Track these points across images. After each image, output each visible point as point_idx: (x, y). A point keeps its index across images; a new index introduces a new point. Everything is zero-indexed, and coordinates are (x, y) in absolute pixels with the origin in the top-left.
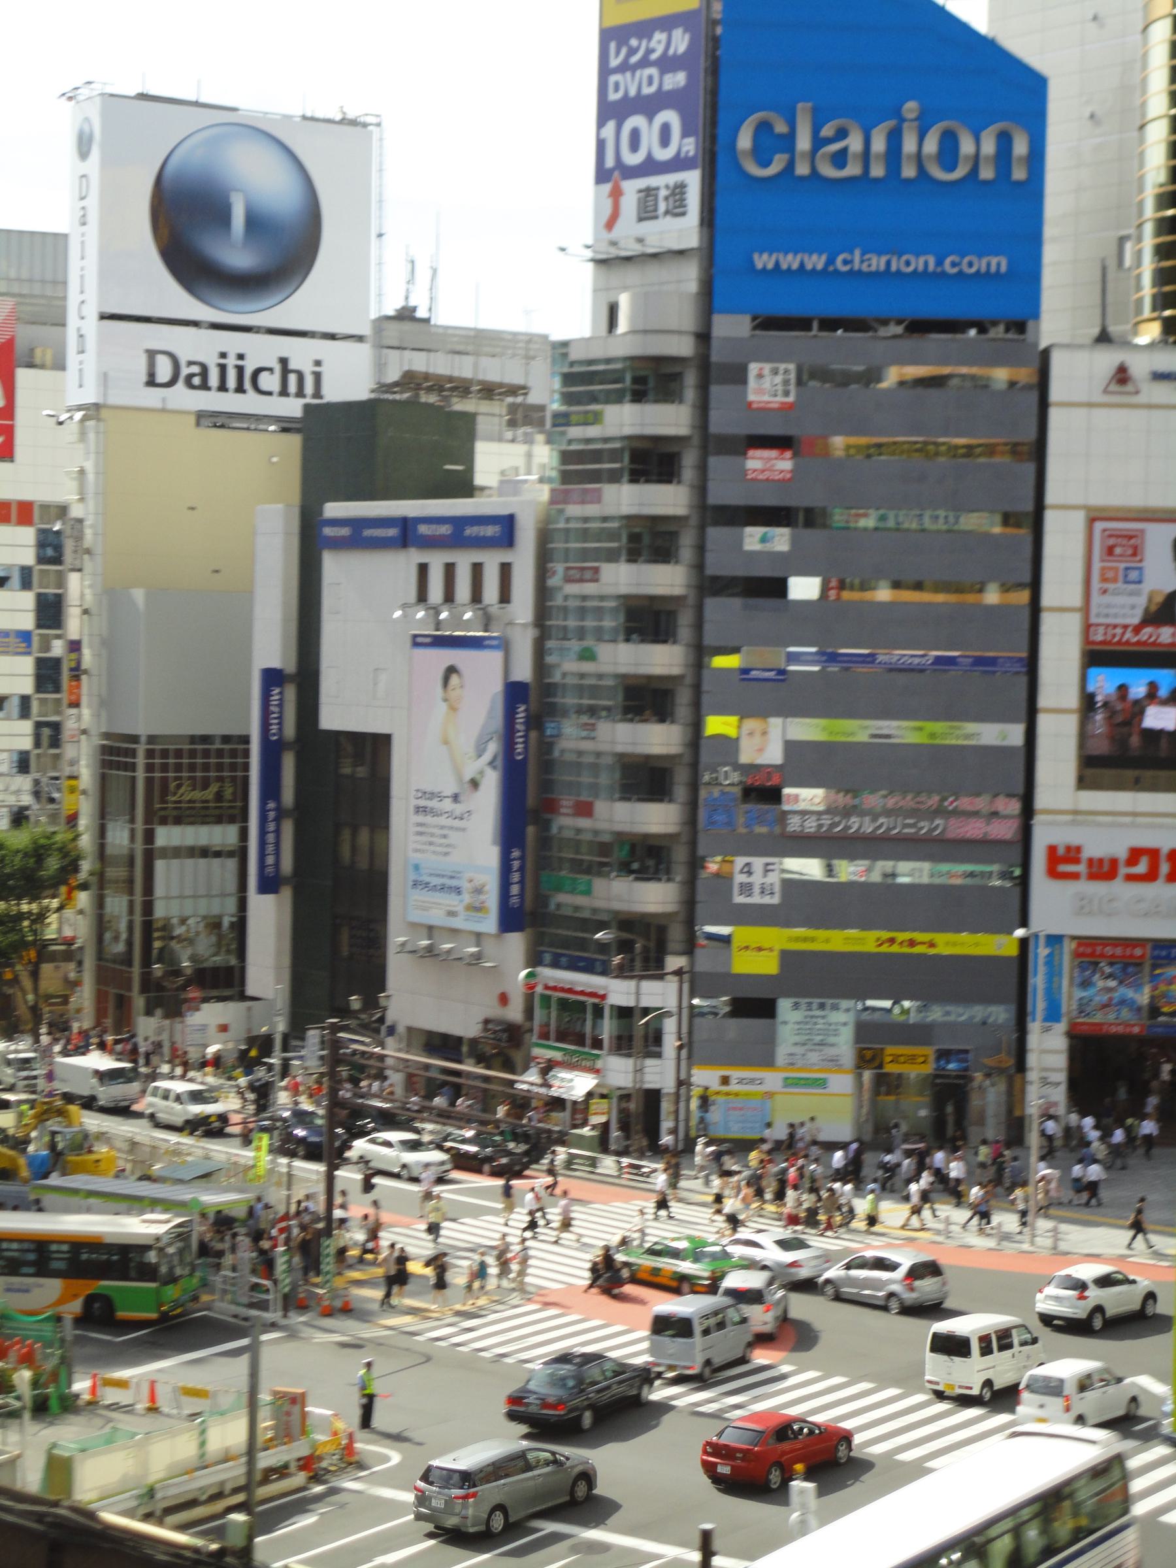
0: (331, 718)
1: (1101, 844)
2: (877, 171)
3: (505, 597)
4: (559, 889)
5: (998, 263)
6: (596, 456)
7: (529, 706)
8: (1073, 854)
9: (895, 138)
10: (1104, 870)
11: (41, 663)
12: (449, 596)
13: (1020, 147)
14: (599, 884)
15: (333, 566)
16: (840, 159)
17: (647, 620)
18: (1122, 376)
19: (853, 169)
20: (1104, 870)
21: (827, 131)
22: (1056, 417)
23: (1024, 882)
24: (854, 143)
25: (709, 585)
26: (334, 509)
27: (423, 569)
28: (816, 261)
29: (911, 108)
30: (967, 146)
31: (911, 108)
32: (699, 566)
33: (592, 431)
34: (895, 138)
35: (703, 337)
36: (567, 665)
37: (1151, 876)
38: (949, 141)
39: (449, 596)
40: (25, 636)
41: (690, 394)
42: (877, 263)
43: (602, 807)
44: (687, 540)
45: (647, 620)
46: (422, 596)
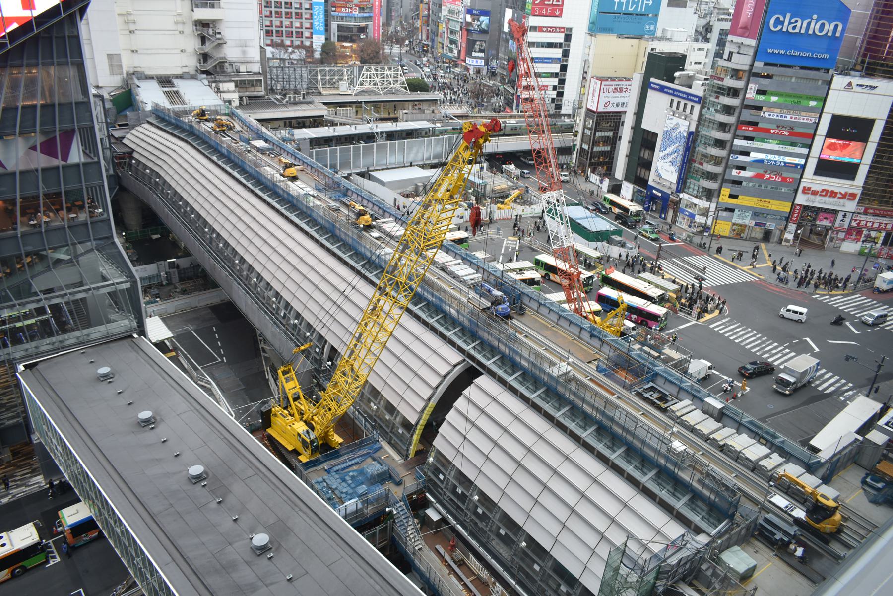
2: (803, 31)
3: (691, 113)
5: (827, 56)
6: (720, 88)
7: (693, 138)
8: (809, 188)
9: (809, 24)
10: (815, 193)
12: (677, 108)
13: (840, 28)
15: (650, 93)
16: (794, 28)
17: (723, 127)
18: (850, 84)
19: (797, 30)
20: (815, 193)
21: (793, 21)
22: (831, 92)
23: (796, 191)
24: (799, 24)
25: (741, 123)
26: (652, 80)
27: (672, 101)
28: (783, 52)
29: (815, 17)
30: (827, 27)
31: (815, 17)
32: (739, 117)
33: (720, 83)
34: (809, 24)
35: (752, 65)
36: (704, 131)
37: (825, 195)
38: (823, 25)
39: (677, 108)
40: (559, 59)
41: (745, 79)
42: (797, 53)
43: (705, 164)
44: (737, 111)
45: (723, 127)
46: (671, 106)
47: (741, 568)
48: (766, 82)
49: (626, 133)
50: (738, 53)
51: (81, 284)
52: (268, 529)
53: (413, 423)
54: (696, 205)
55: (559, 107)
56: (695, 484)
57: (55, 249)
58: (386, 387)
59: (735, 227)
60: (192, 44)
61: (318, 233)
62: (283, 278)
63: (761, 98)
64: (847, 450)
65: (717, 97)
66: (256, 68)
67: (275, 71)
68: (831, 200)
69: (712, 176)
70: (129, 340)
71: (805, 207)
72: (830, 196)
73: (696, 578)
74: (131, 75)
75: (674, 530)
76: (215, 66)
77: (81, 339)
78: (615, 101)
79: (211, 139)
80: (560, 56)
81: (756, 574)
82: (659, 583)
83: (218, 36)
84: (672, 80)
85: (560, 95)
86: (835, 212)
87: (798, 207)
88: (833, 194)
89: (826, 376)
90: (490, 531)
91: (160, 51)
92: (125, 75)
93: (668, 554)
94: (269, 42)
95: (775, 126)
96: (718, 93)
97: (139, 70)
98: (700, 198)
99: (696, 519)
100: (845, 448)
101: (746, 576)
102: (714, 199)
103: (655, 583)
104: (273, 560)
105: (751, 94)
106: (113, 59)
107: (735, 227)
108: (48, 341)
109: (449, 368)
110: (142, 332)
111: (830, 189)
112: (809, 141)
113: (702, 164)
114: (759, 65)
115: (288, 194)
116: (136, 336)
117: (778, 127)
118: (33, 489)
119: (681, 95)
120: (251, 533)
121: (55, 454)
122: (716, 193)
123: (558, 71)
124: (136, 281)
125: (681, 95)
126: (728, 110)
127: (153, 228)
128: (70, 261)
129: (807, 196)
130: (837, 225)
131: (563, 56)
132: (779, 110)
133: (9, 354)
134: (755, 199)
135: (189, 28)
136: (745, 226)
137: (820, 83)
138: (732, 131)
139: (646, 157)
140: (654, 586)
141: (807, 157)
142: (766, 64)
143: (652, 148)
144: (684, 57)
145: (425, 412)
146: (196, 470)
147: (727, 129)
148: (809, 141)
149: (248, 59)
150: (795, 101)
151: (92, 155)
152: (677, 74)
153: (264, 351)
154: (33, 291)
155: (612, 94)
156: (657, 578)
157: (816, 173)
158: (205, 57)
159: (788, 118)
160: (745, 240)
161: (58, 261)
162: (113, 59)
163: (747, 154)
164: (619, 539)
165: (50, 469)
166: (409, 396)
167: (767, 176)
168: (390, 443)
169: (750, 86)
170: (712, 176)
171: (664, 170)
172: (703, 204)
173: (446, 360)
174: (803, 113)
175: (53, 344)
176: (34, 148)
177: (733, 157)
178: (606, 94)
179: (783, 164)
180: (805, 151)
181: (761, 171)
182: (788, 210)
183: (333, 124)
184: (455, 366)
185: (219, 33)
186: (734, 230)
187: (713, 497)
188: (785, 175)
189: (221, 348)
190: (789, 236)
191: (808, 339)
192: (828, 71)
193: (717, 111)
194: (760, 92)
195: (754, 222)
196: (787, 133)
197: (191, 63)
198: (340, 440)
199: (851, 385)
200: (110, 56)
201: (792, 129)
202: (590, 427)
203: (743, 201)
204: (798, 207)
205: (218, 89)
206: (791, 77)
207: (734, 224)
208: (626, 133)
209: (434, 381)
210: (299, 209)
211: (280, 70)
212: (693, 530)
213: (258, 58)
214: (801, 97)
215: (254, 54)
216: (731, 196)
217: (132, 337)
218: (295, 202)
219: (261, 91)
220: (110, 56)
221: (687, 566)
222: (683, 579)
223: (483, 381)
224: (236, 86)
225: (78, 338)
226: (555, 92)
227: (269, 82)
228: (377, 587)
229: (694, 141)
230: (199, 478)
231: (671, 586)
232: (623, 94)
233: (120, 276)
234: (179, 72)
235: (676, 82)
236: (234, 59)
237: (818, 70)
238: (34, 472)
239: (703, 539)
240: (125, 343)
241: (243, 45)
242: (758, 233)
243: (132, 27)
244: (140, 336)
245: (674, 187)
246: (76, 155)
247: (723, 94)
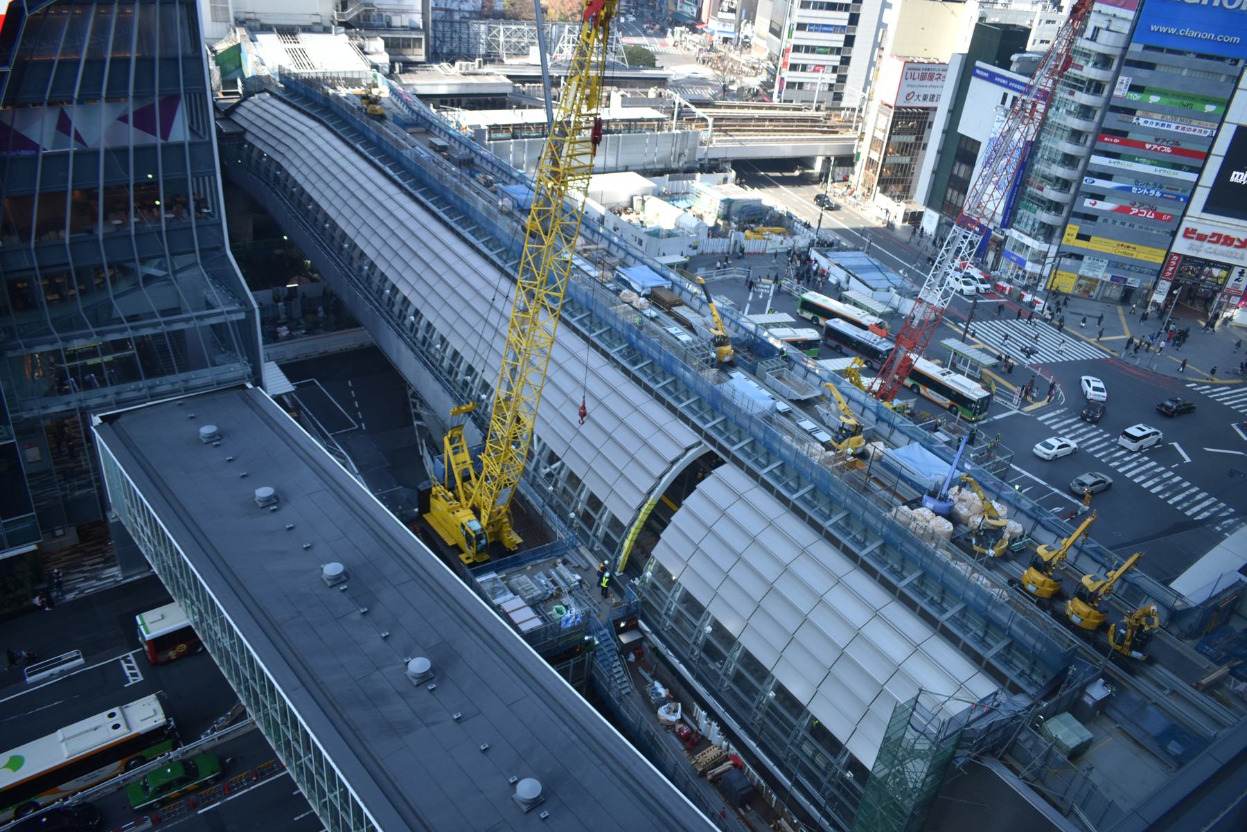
0: (962, 129)
1: (1202, 230)
4: (1026, 207)
6: (1076, 80)
7: (1031, 148)
8: (1194, 231)
10: (1202, 238)
11: (847, 37)
14: (1039, 212)
15: (976, 85)
17: (1076, 135)
20: (1202, 238)
25: (1103, 132)
26: (978, 64)
27: (1005, 96)
28: (1173, 31)
32: (1101, 122)
35: (1126, 48)
37: (1217, 242)
40: (844, 27)
42: (1194, 34)
44: (1099, 113)
46: (1003, 102)
47: (1072, 741)
48: (1144, 73)
49: (934, 138)
50: (1108, 29)
51: (177, 310)
52: (427, 653)
53: (626, 524)
54: (1028, 247)
55: (838, 97)
56: (1014, 627)
57: (143, 261)
58: (590, 474)
59: (1083, 282)
61: (500, 258)
62: (451, 318)
63: (1135, 97)
64: (1228, 594)
65: (1072, 93)
67: (440, 26)
68: (1225, 248)
69: (1056, 207)
70: (240, 391)
71: (1185, 257)
72: (1223, 244)
73: (1009, 751)
75: (984, 687)
77: (177, 386)
78: (922, 91)
79: (354, 119)
80: (845, 23)
81: (1091, 752)
82: (959, 752)
84: (1006, 65)
85: (842, 79)
86: (1229, 268)
87: (1176, 258)
88: (1228, 241)
89: (1198, 497)
90: (725, 674)
93: (972, 717)
95: (1152, 140)
96: (1074, 87)
97: (252, 16)
98: (1035, 238)
99: (1012, 675)
100: (1225, 591)
101: (1076, 754)
102: (1055, 240)
103: (954, 752)
104: (435, 692)
105: (1121, 91)
107: (1083, 282)
108: (133, 385)
109: (678, 452)
110: (258, 382)
111: (1225, 232)
112: (1198, 163)
113: (1041, 189)
114: (1136, 48)
115: (462, 201)
116: (249, 386)
117: (1157, 140)
118: (106, 584)
119: (1019, 87)
120: (406, 656)
121: (139, 538)
122: (1058, 233)
123: (841, 45)
124: (253, 310)
125: (1019, 87)
126: (1085, 112)
127: (279, 239)
128: (164, 279)
129: (1190, 241)
130: (1229, 285)
131: (850, 23)
132: (1159, 116)
133: (80, 400)
134: (1115, 243)
136: (1097, 280)
137: (1223, 79)
138: (1088, 143)
139: (961, 175)
140: (953, 757)
141: (1196, 184)
142: (1147, 48)
143: (971, 162)
144: (1027, 31)
145: (643, 510)
146: (332, 569)
147: (1082, 140)
148: (1198, 163)
150: (1186, 102)
151: (201, 133)
152: (1014, 57)
153: (419, 417)
154: (114, 316)
155: (917, 82)
156: (957, 746)
157: (1206, 209)
159: (1173, 128)
160: (1096, 300)
161: (149, 279)
163: (1107, 177)
164: (903, 696)
165: (133, 558)
166: (621, 488)
167: (1135, 210)
168: (591, 550)
169: (1120, 78)
170: (1056, 207)
171: (988, 195)
172: (1036, 245)
173: (677, 441)
174: (1195, 122)
175: (140, 390)
176: (124, 119)
177: (1087, 181)
178: (910, 82)
179: (1158, 194)
180: (1193, 177)
181: (1127, 204)
182: (1160, 260)
183: (521, 107)
184: (688, 449)
186: (1080, 286)
187: (1039, 646)
188: (1160, 210)
189: (358, 410)
190: (1159, 298)
191: (1176, 444)
192: (1237, 62)
193: (1069, 112)
194: (1133, 88)
195: (1109, 276)
196: (1168, 150)
198: (520, 540)
199: (1232, 510)
201: (1177, 144)
202: (872, 543)
203: (1096, 244)
204: (1176, 258)
206: (1183, 68)
207: (1081, 277)
208: (934, 138)
209: (657, 469)
210: (477, 223)
211: (448, 25)
212: (1009, 688)
214: (1193, 99)
216: (1080, 237)
217: (244, 387)
218: (471, 214)
221: (999, 734)
222: (992, 752)
223: (726, 471)
224: (386, 46)
225: (173, 384)
226: (835, 76)
227: (431, 43)
228: (574, 737)
229: (1032, 155)
230: (337, 580)
231: (976, 758)
232: (934, 83)
233: (231, 303)
234: (307, 21)
235: (1013, 68)
237: (1222, 59)
238: (109, 562)
239: (1022, 701)
240: (235, 392)
242: (1115, 292)
244: (255, 385)
245: (999, 219)
246: (180, 132)
247: (1081, 89)
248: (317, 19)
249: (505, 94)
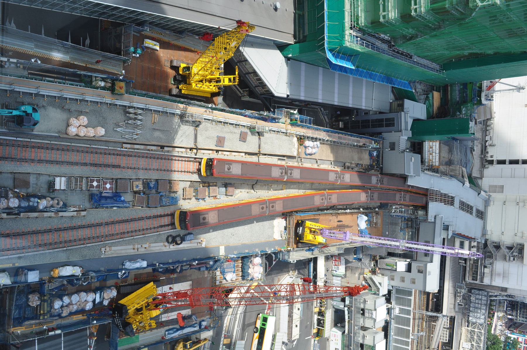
60: (507, 240)
66: (487, 281)
74: (490, 196)
76: (490, 252)
83: (512, 258)
91: (503, 219)
92: (488, 193)
94: (520, 340)
97: (492, 203)
106: (501, 189)
135: (518, 240)
149: (494, 277)
158: (498, 247)
162: (501, 189)
185: (514, 260)
197: (494, 236)
200: (502, 187)
205: (472, 247)
211: (485, 302)
213: (494, 284)
215: (498, 282)
219: (469, 279)
220: (502, 187)
234: (489, 228)
236: (494, 267)
241: (505, 275)
243: (521, 204)
248: (489, 233)
249: (442, 312)
